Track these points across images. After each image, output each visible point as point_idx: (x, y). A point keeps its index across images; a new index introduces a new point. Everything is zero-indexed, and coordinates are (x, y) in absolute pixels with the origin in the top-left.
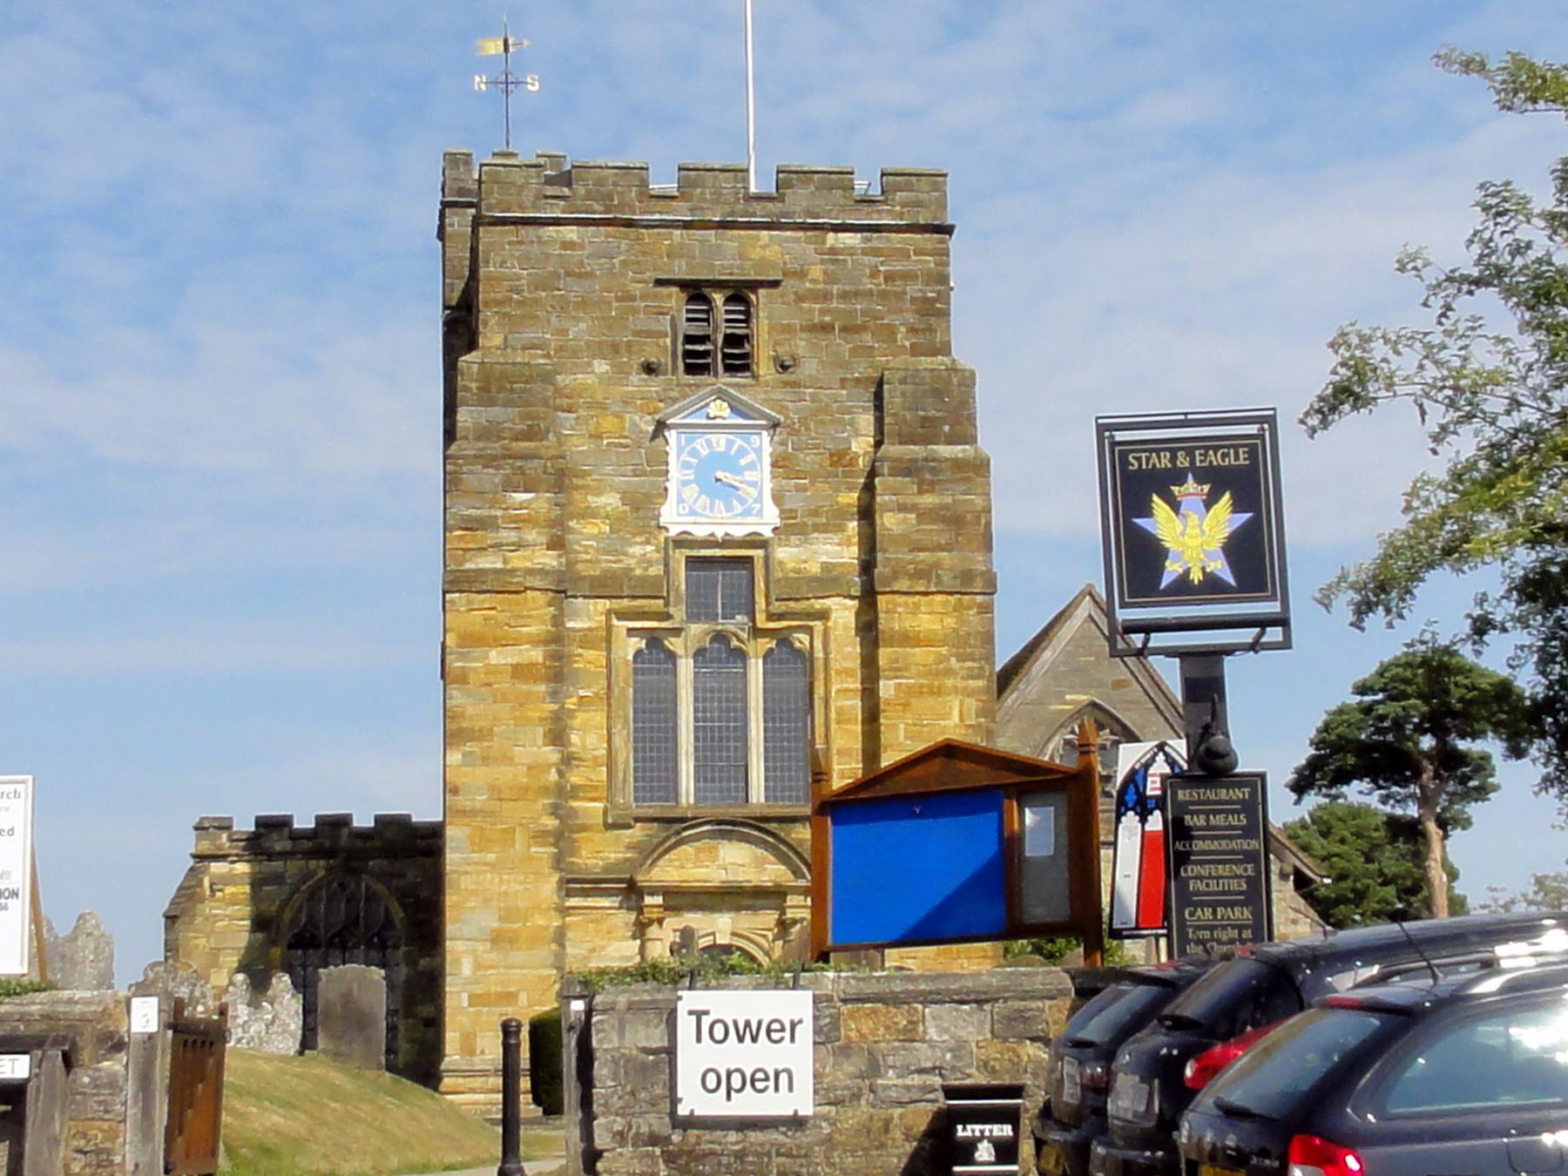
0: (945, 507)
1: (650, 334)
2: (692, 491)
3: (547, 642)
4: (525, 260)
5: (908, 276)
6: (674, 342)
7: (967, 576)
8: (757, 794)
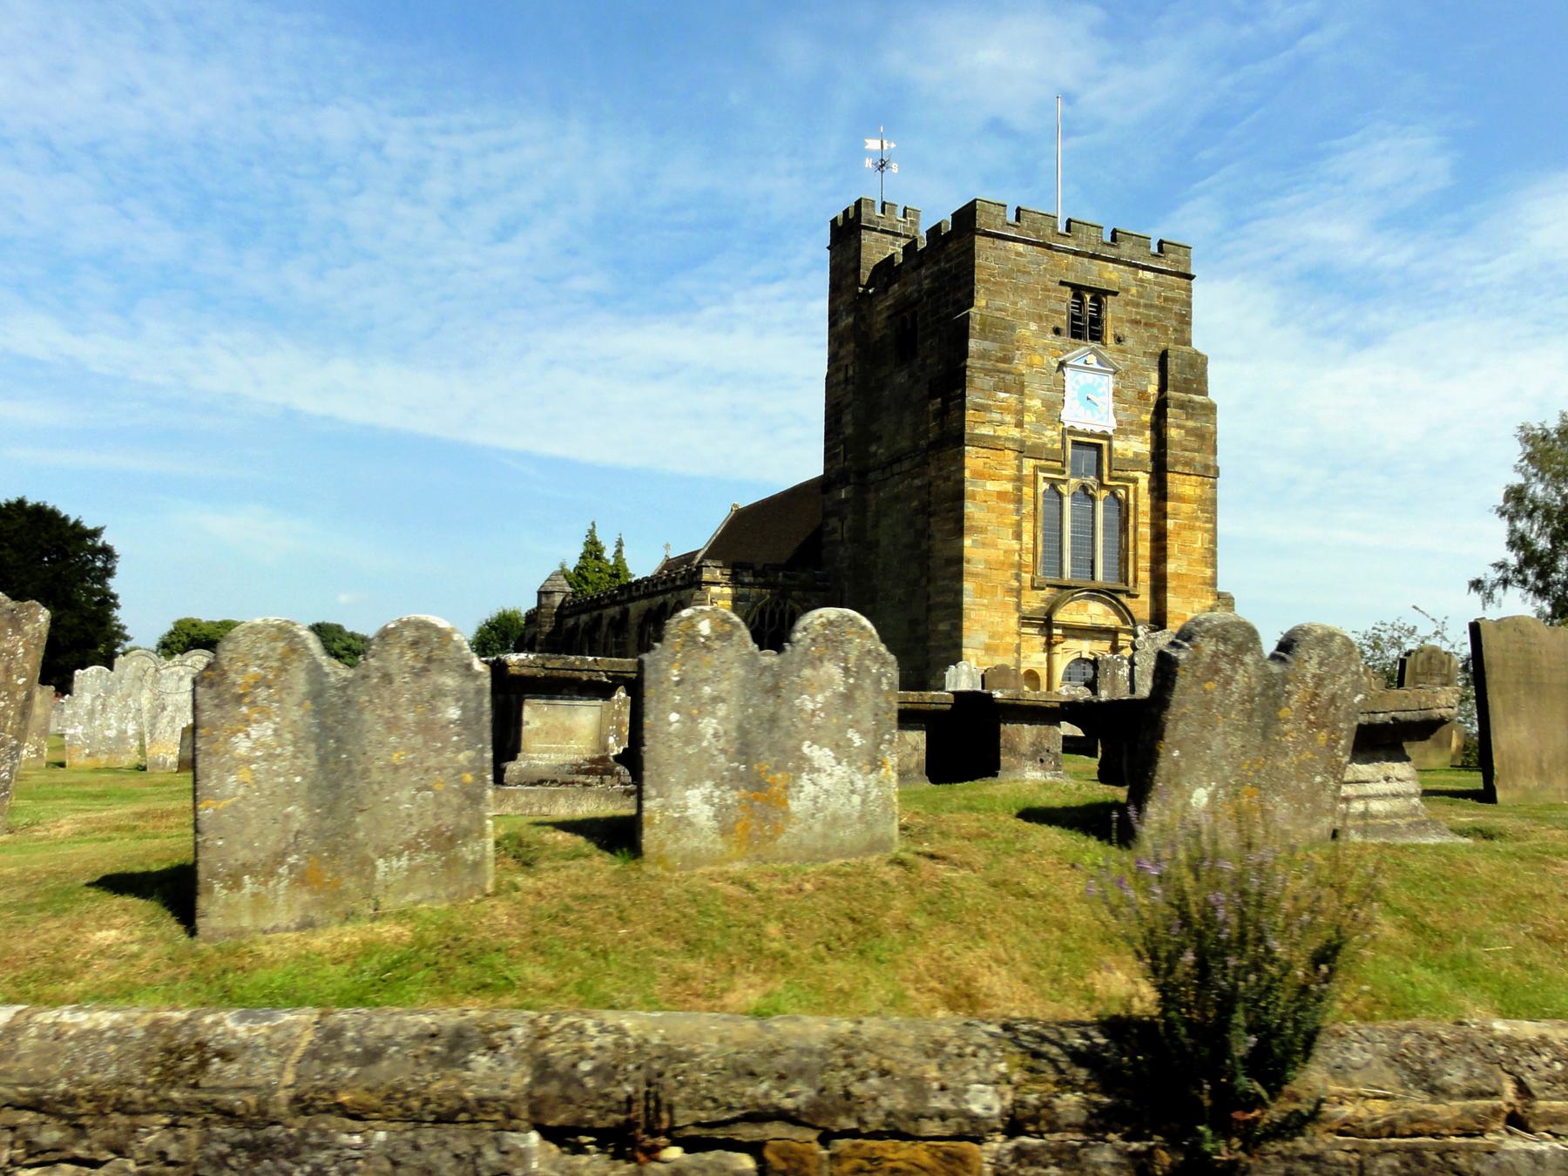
4: (997, 259)
5: (1174, 300)
7: (1207, 467)
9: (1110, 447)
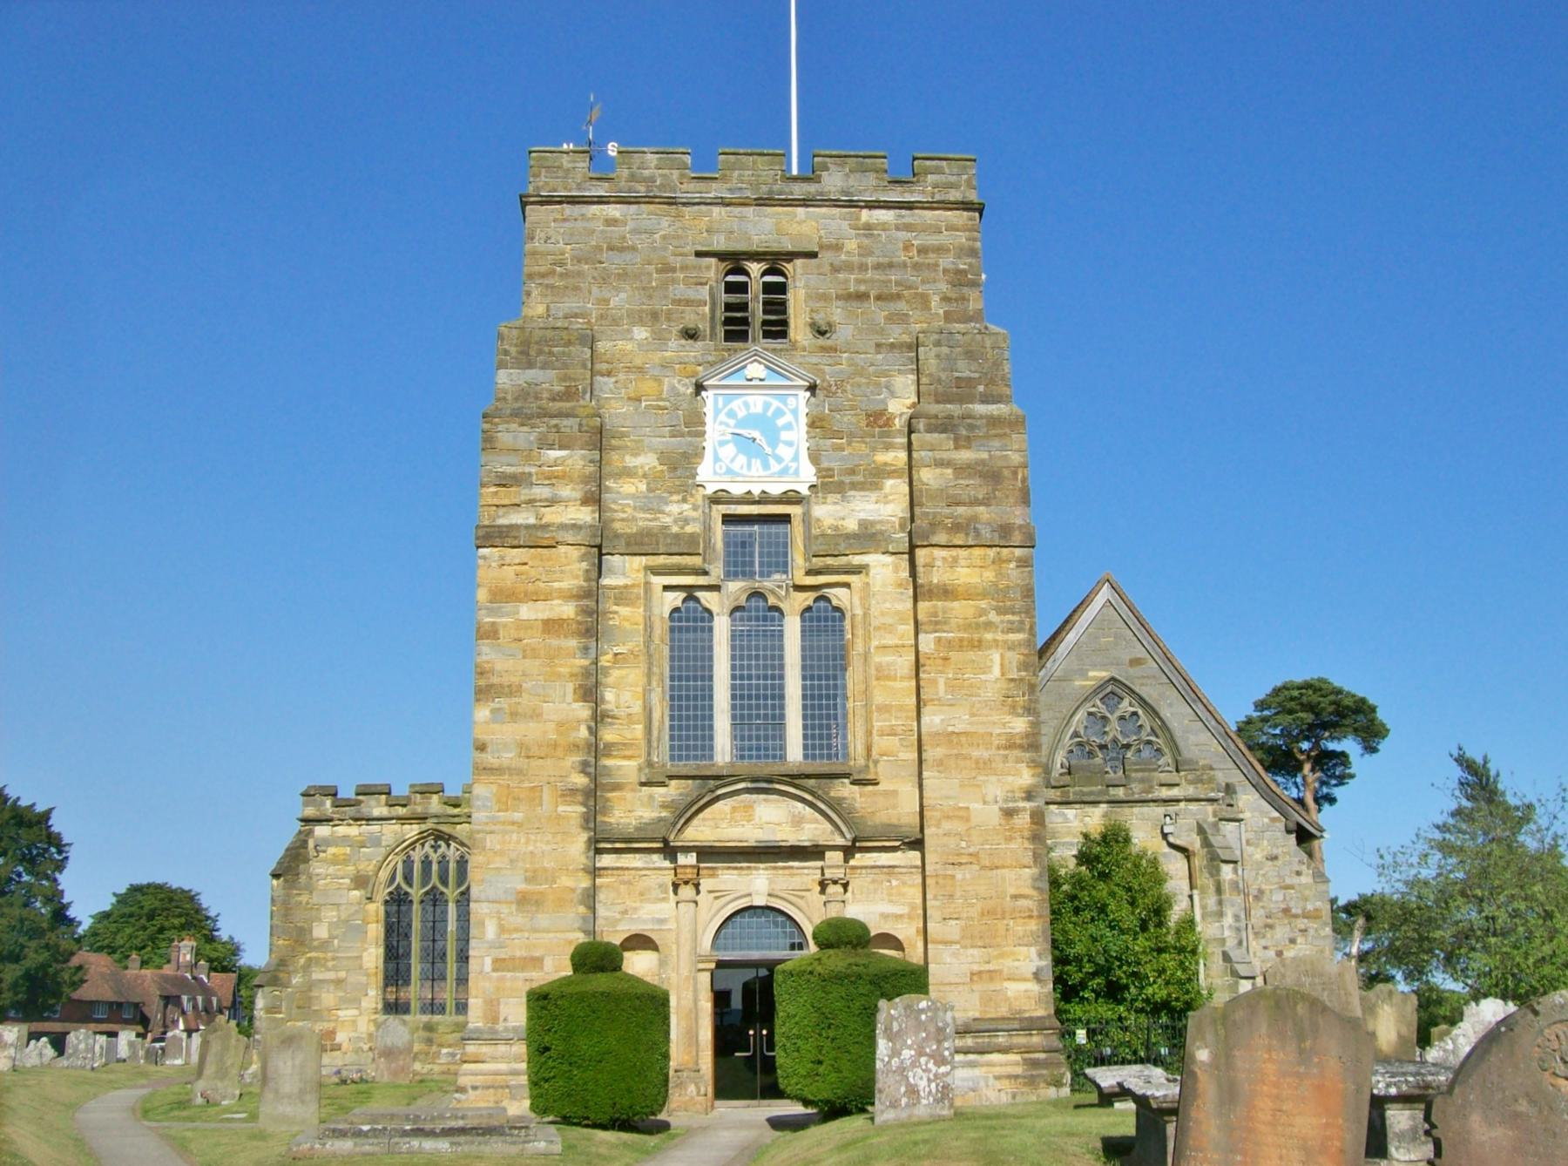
0: (983, 462)
1: (689, 302)
2: (729, 451)
3: (579, 597)
5: (940, 250)
6: (713, 311)
7: (1005, 530)
8: (795, 752)
9: (807, 519)
